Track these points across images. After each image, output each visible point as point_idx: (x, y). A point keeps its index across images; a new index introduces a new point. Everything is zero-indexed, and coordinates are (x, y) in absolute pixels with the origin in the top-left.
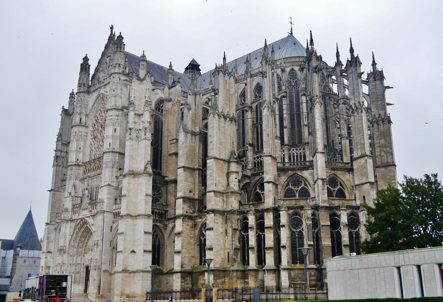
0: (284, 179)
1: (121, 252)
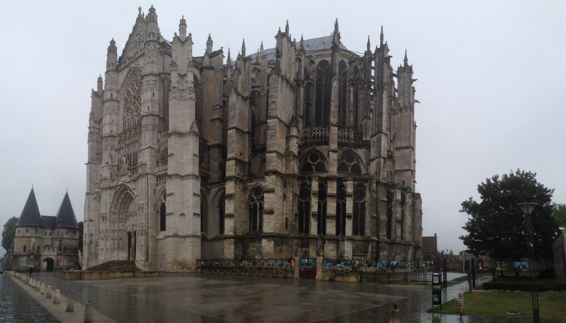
1: (172, 214)
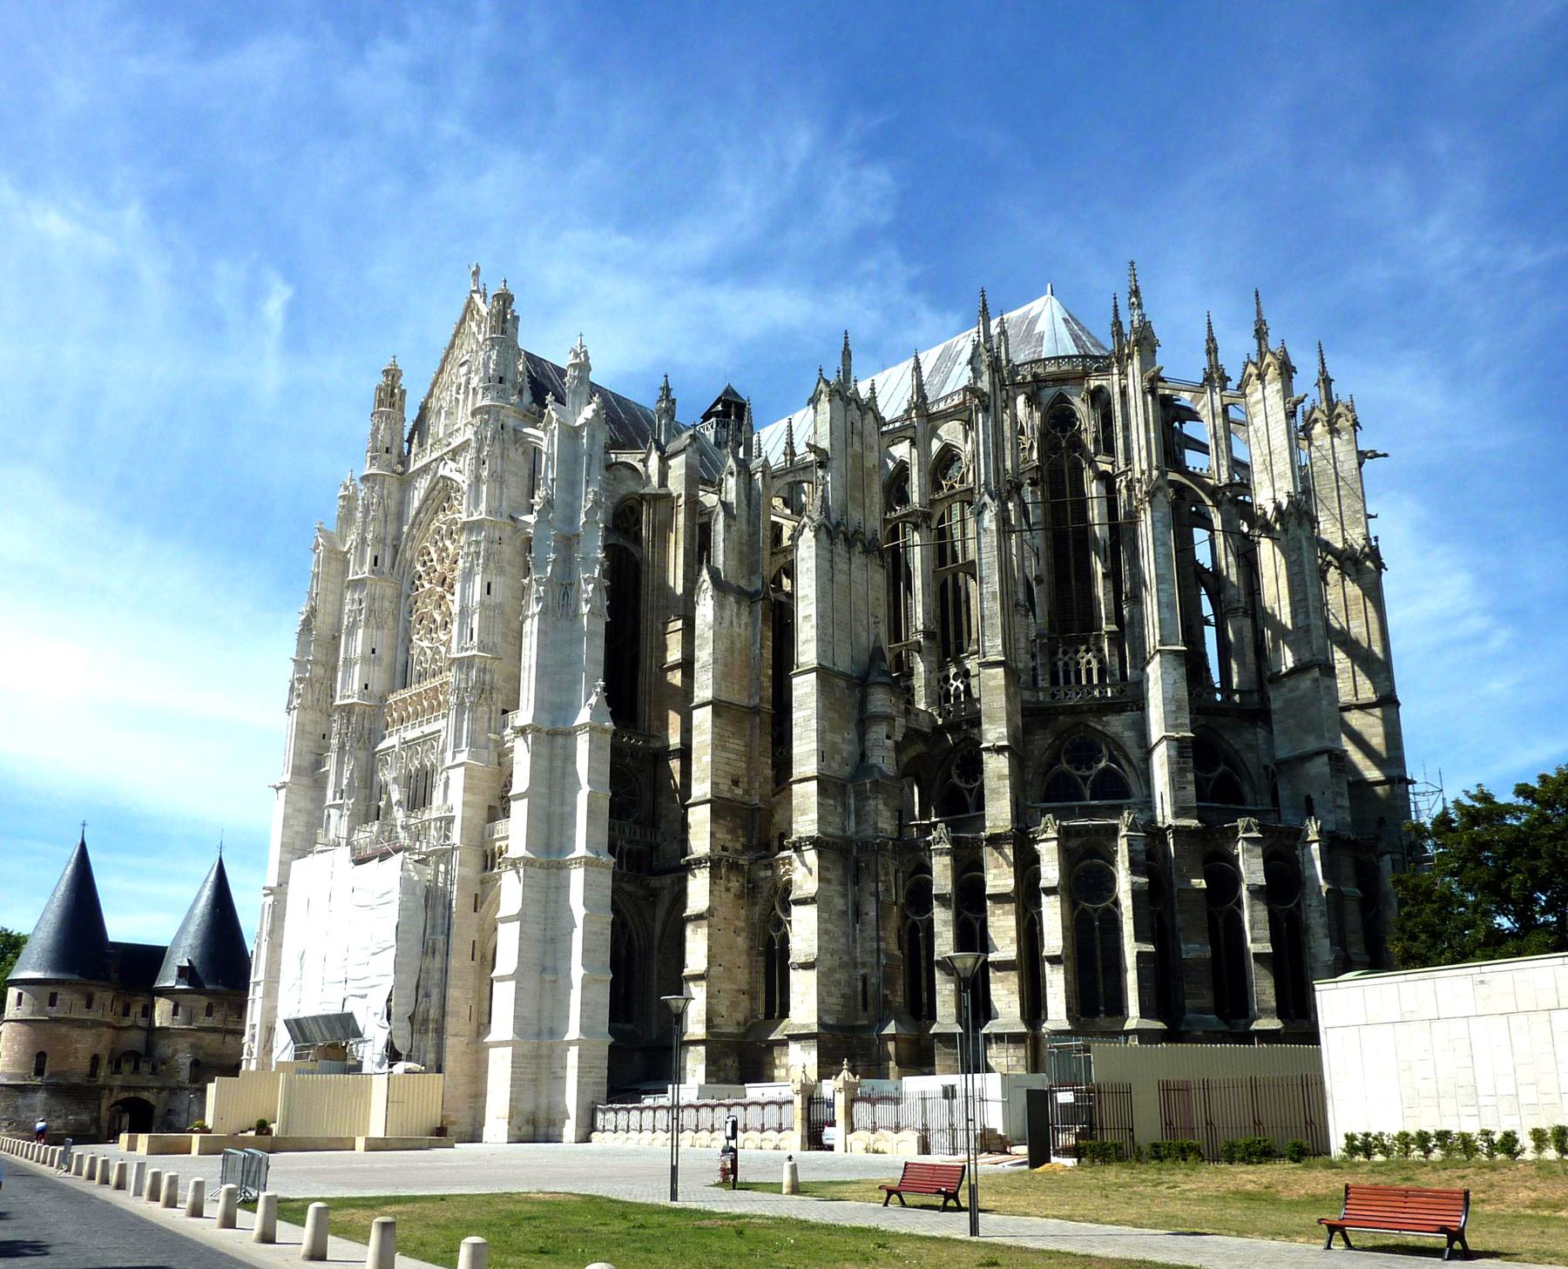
0: (1042, 741)
